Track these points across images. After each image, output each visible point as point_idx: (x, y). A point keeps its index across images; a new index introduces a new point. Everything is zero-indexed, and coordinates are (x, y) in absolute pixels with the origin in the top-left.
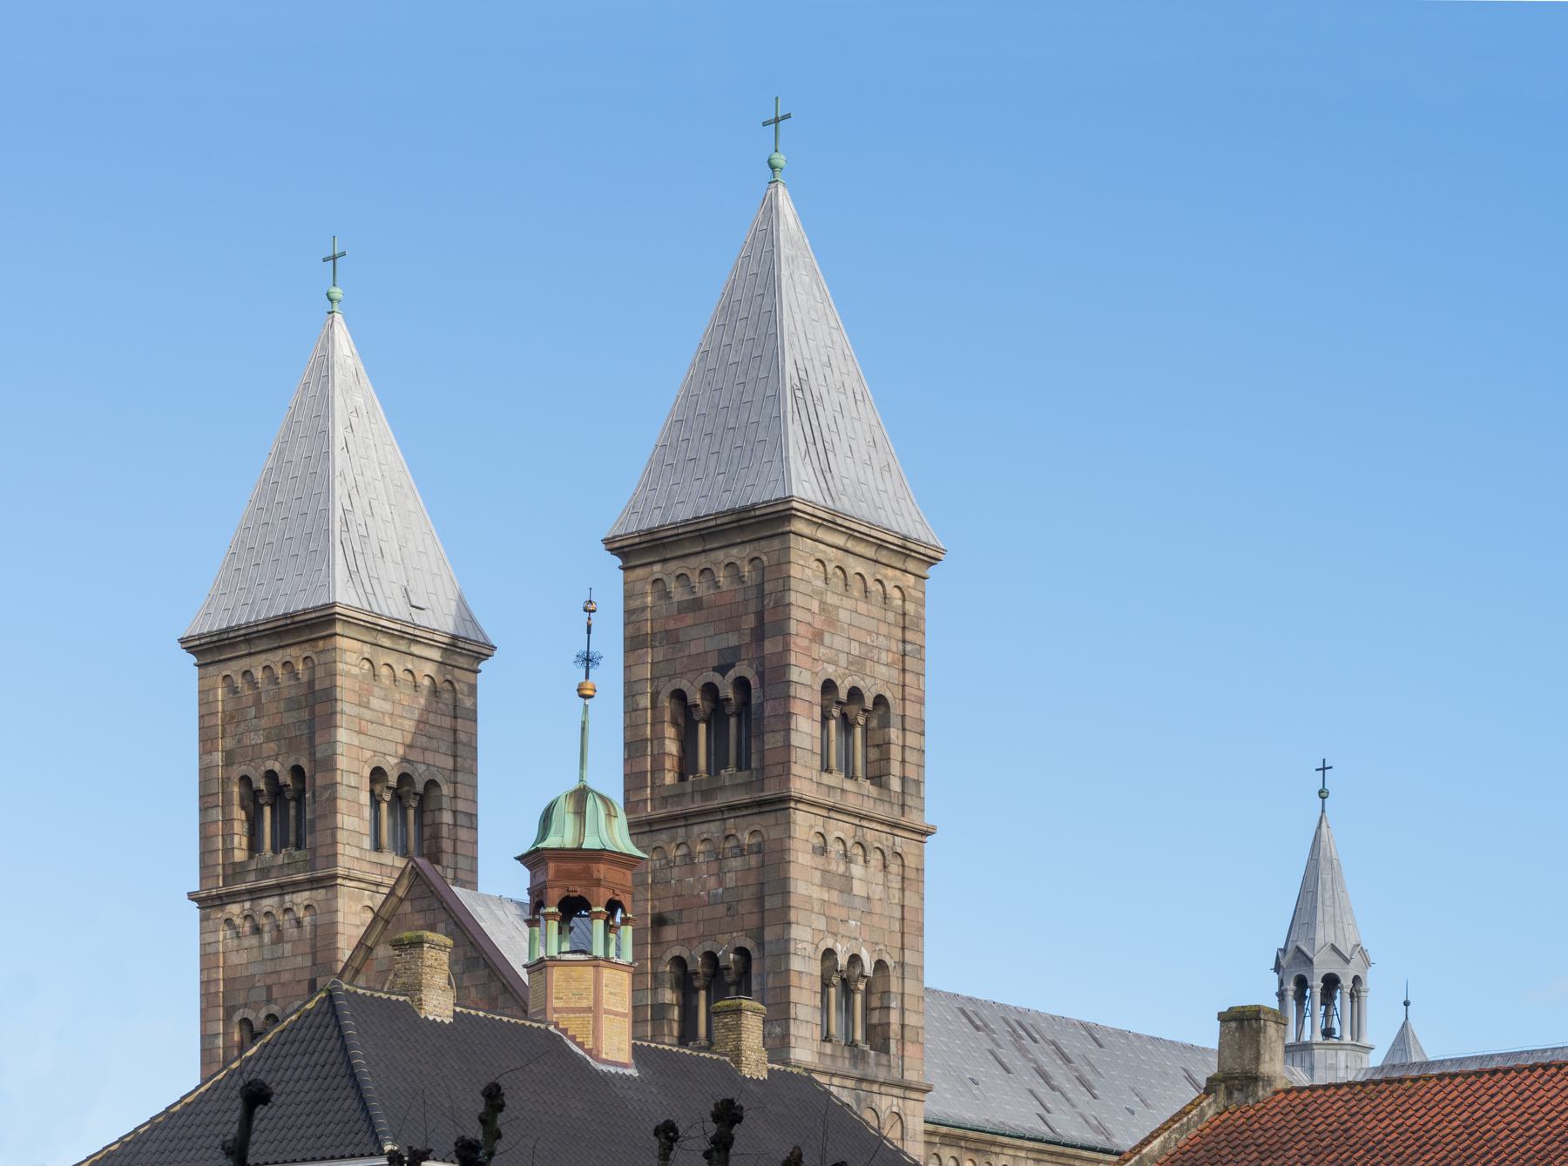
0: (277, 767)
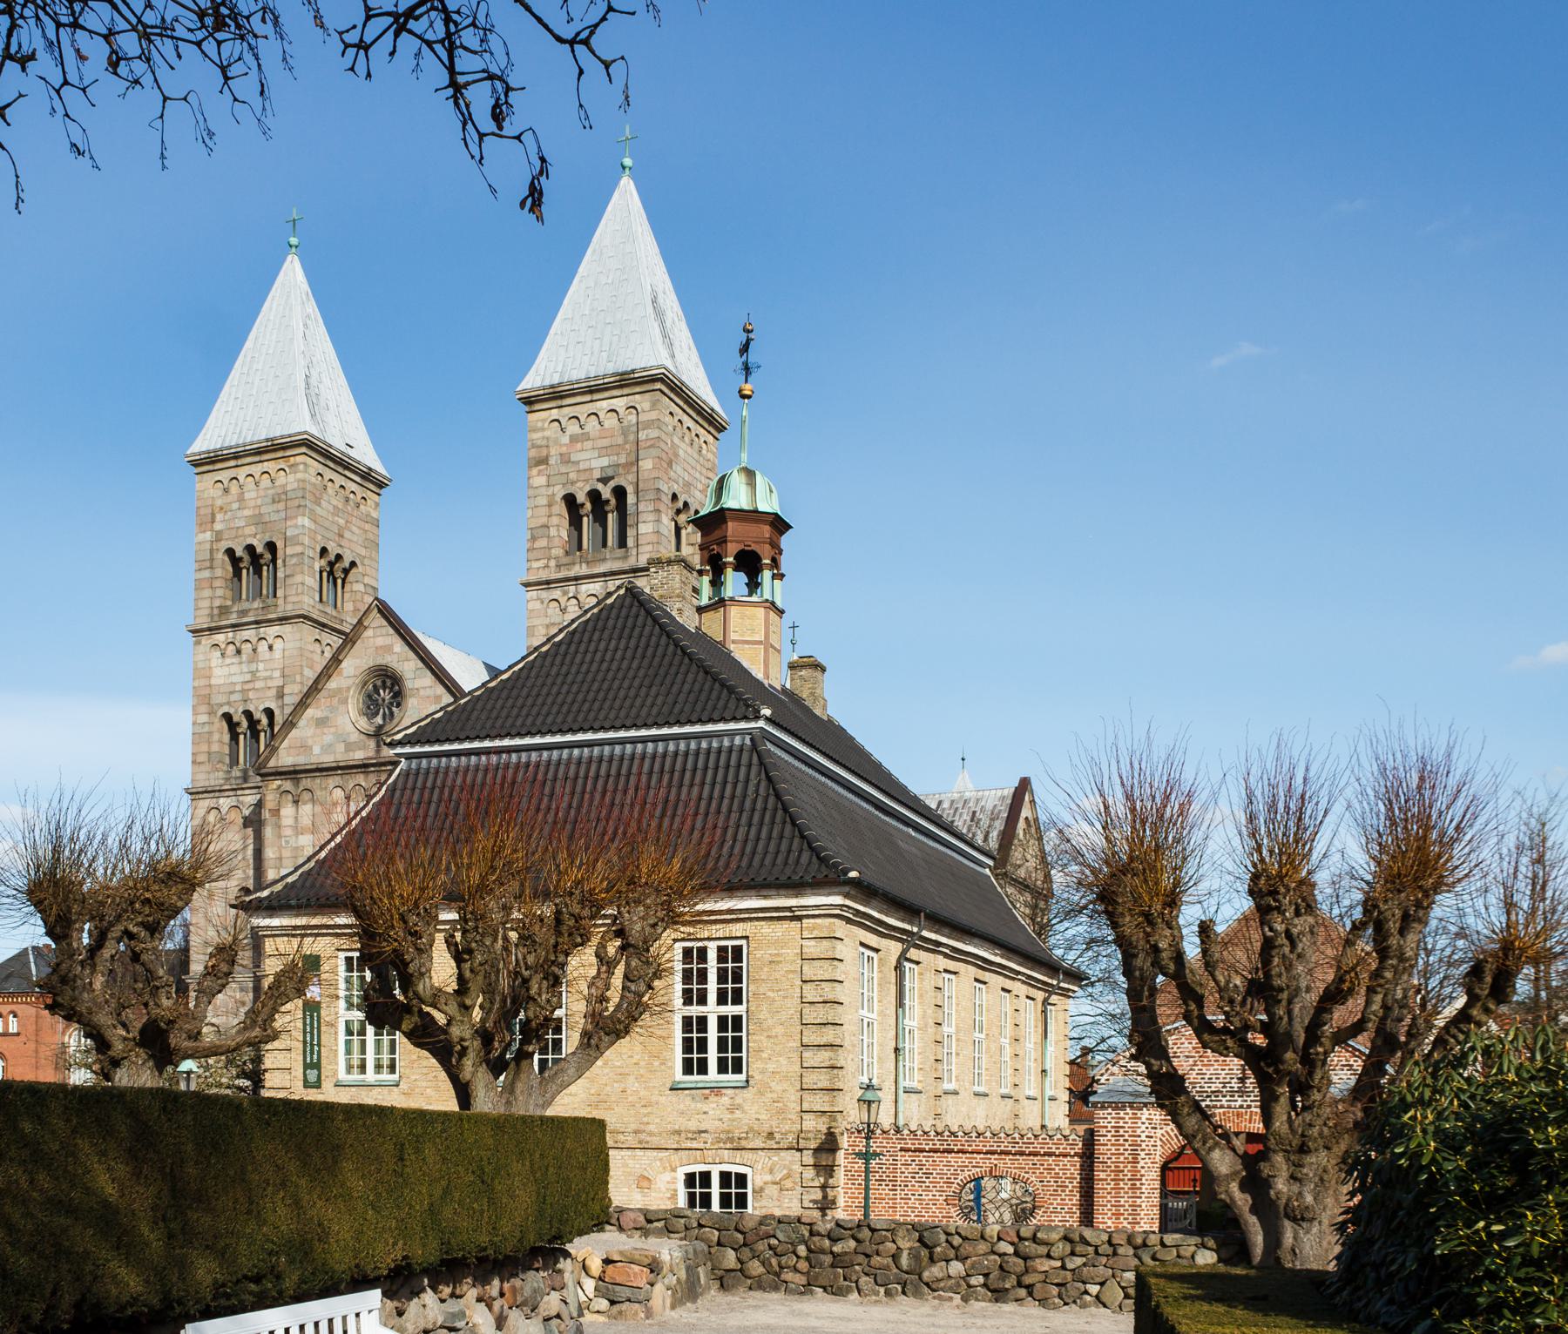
0: (255, 542)
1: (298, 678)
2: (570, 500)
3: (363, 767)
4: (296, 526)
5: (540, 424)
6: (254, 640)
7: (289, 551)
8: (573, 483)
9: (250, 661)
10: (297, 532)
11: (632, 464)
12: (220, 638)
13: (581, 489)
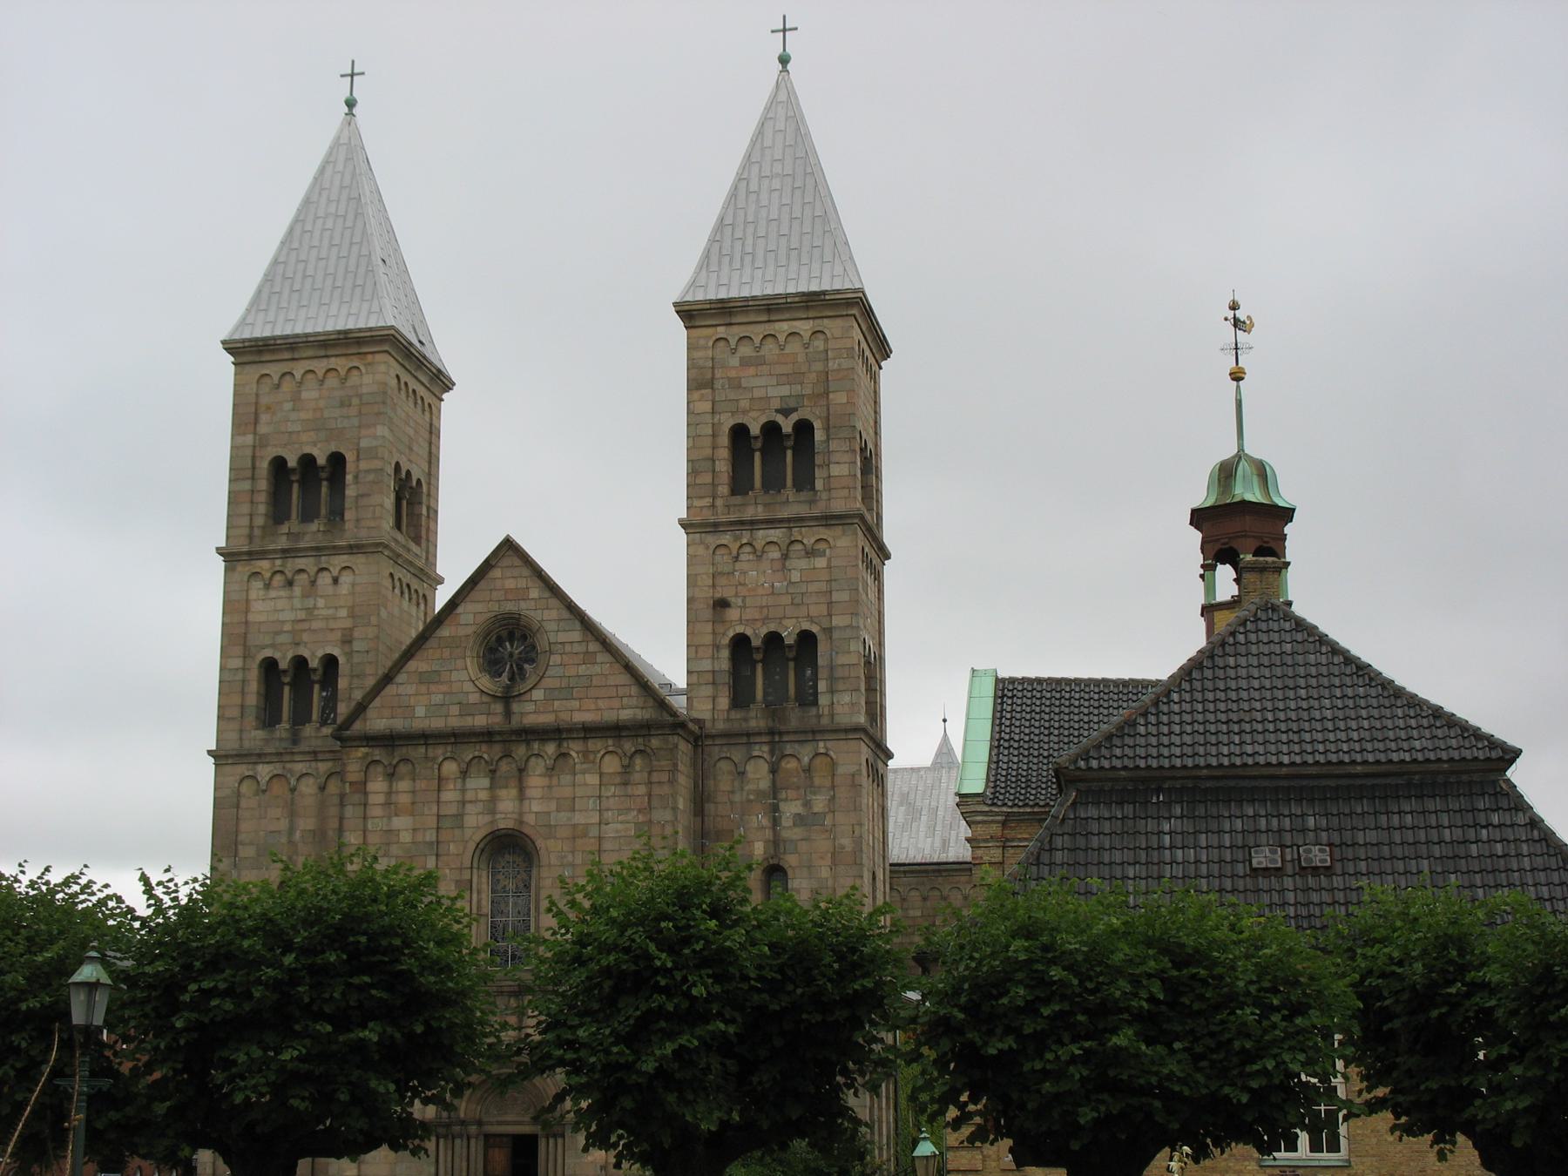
0: (315, 452)
1: (374, 620)
3: (487, 736)
4: (375, 437)
5: (702, 342)
6: (312, 570)
7: (363, 465)
8: (745, 412)
10: (374, 443)
12: (264, 565)
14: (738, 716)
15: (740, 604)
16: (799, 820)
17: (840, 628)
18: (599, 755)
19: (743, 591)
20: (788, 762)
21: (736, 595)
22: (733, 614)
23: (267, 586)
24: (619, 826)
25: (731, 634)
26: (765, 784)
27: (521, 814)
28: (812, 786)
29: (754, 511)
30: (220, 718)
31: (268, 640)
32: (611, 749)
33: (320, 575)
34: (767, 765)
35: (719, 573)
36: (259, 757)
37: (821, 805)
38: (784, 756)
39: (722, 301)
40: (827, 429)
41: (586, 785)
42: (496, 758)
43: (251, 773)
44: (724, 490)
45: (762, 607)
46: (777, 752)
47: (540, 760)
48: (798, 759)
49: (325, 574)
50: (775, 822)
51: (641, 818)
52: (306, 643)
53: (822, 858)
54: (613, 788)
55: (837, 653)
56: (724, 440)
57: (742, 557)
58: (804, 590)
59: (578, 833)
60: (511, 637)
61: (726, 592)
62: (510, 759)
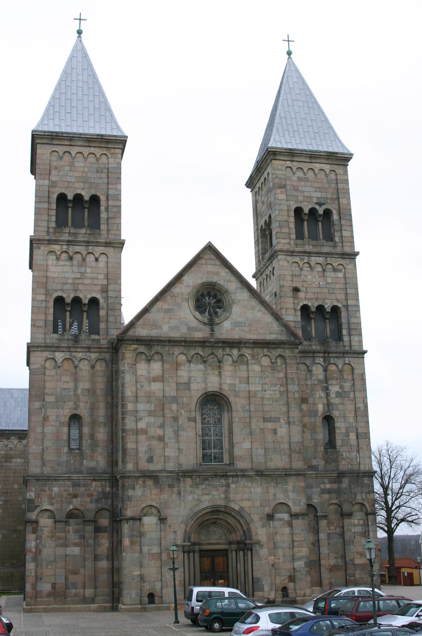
2: (298, 211)
3: (202, 343)
5: (280, 167)
8: (301, 202)
9: (80, 266)
11: (335, 199)
13: (306, 206)
14: (307, 344)
15: (305, 290)
16: (338, 394)
17: (352, 305)
18: (260, 357)
19: (305, 285)
20: (332, 367)
21: (302, 286)
22: (301, 295)
23: (58, 259)
24: (272, 393)
25: (301, 304)
26: (321, 377)
27: (221, 384)
28: (343, 378)
29: (308, 248)
30: (33, 326)
31: (59, 287)
32: (266, 353)
33: (88, 256)
34: (322, 368)
35: (294, 275)
36: (56, 348)
37: (348, 388)
38: (330, 364)
39: (291, 149)
40: (339, 214)
41: (254, 371)
42: (207, 355)
43: (52, 357)
44: (293, 236)
45: (315, 293)
46: (327, 362)
47: (229, 357)
48: (337, 366)
49: (91, 255)
50: (328, 395)
51: (282, 389)
52: (81, 290)
53: (350, 413)
54: (267, 374)
55: (351, 317)
56: (292, 214)
57: (304, 269)
58: (334, 287)
59: (250, 396)
60: (209, 294)
61: (299, 285)
62: (213, 356)
